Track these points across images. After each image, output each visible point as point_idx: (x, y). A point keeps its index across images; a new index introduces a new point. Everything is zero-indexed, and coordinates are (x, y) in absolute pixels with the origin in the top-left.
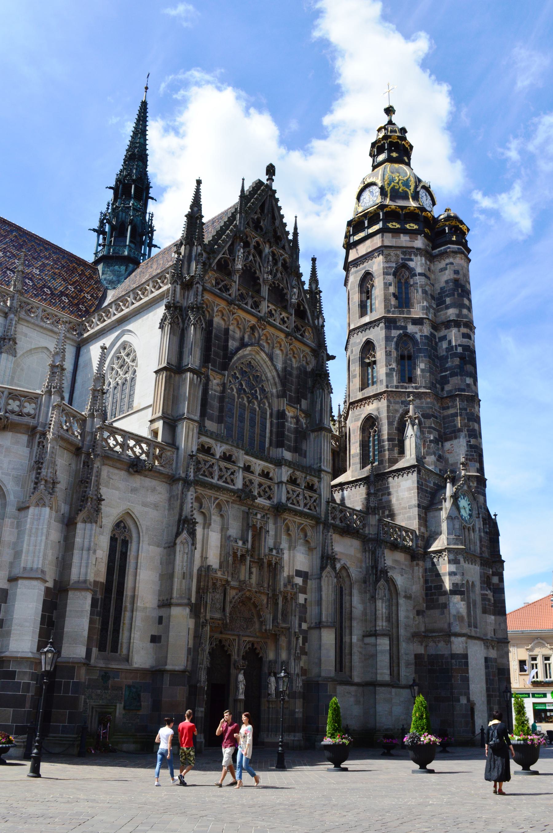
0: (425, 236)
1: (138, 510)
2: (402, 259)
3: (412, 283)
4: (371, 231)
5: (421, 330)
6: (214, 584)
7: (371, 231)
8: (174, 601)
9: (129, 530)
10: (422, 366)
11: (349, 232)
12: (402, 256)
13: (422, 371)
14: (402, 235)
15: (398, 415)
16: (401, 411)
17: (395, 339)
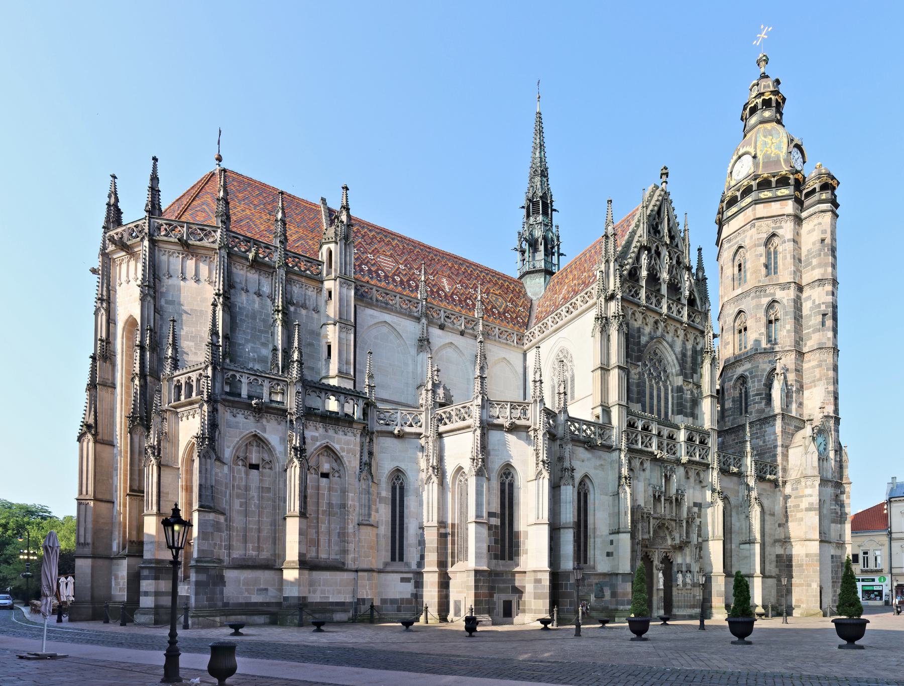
0: (795, 201)
1: (592, 473)
2: (773, 228)
3: (781, 250)
4: (743, 204)
5: (788, 295)
6: (642, 516)
7: (743, 204)
8: (621, 530)
9: (588, 487)
10: (788, 327)
11: (723, 208)
12: (773, 225)
13: (788, 331)
14: (773, 203)
15: (766, 373)
16: (768, 369)
17: (765, 306)
